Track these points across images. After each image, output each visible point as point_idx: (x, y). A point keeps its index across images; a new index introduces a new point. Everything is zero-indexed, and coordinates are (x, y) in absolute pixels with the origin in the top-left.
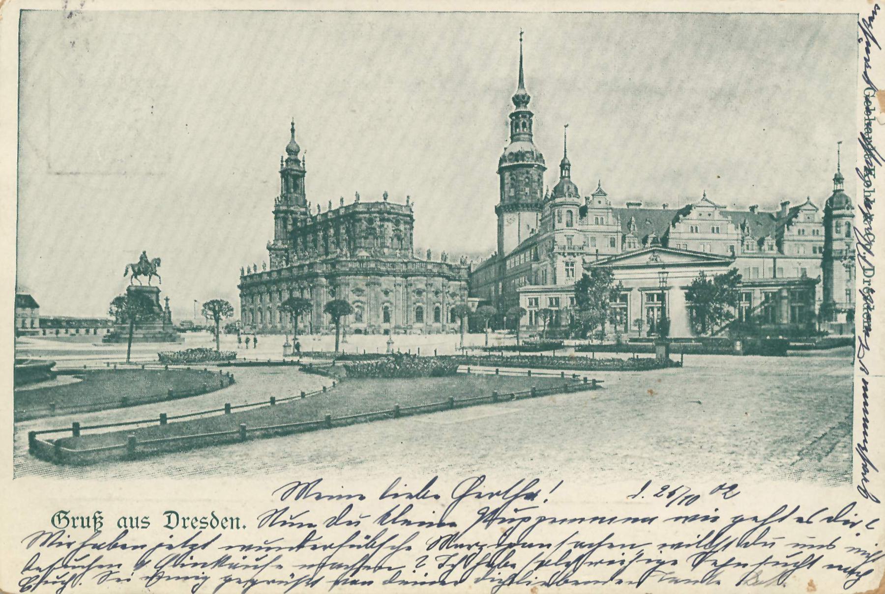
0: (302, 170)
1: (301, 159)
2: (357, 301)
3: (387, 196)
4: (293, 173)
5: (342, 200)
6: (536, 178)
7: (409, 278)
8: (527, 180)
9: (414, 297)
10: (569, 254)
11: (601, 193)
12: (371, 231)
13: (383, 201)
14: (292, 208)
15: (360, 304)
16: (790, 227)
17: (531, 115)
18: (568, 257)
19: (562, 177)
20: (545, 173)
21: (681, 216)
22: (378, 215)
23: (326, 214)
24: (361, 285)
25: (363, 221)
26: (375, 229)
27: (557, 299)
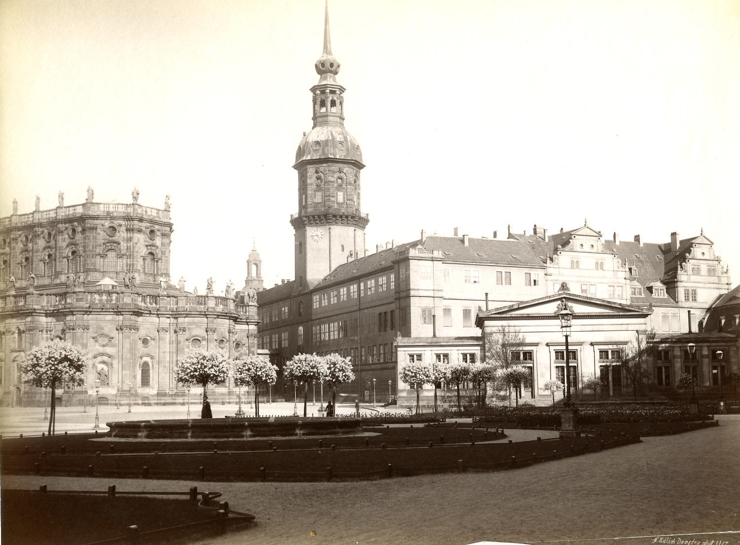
2: (103, 354)
3: (138, 194)
6: (351, 179)
7: (180, 320)
8: (339, 181)
12: (112, 245)
13: (131, 201)
15: (105, 358)
16: (684, 264)
17: (342, 90)
20: (362, 171)
22: (123, 222)
25: (99, 231)
26: (119, 244)
27: (446, 356)
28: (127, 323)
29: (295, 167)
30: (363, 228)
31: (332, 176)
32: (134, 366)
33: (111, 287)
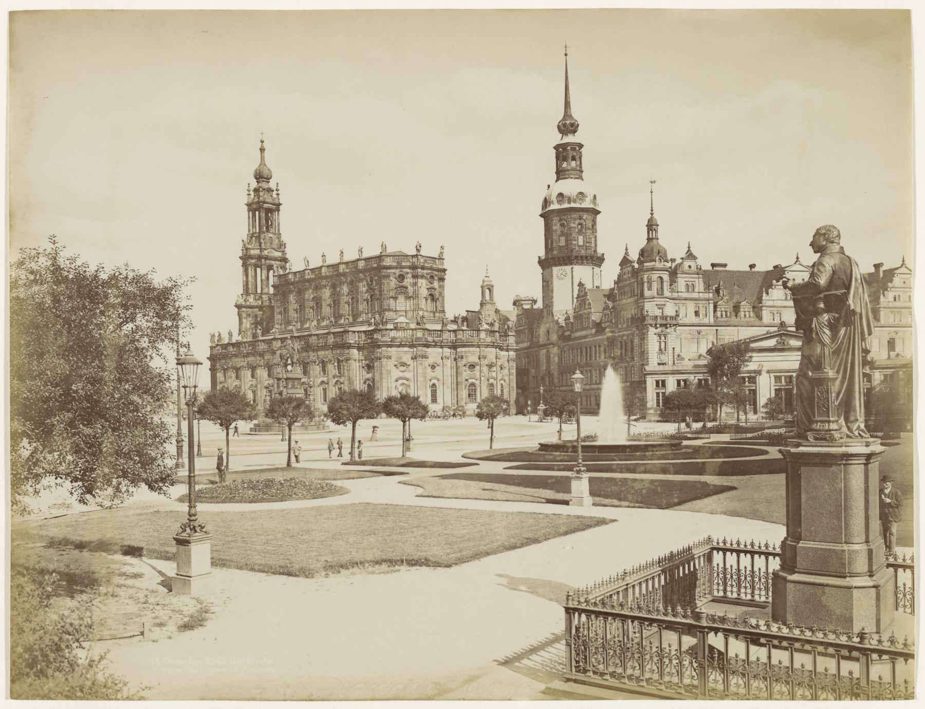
0: (277, 202)
1: (274, 188)
4: (266, 206)
5: (361, 251)
6: (590, 224)
7: (459, 350)
8: (580, 227)
9: (466, 373)
10: (661, 325)
11: (690, 256)
12: (402, 290)
13: (415, 253)
14: (266, 252)
15: (405, 381)
16: (886, 292)
17: (581, 146)
18: (659, 330)
19: (649, 239)
21: (774, 282)
23: (335, 266)
24: (407, 359)
25: (391, 278)
26: (407, 288)
28: (419, 353)
29: (541, 216)
30: (599, 266)
31: (574, 223)
32: (426, 387)
33: (405, 324)
